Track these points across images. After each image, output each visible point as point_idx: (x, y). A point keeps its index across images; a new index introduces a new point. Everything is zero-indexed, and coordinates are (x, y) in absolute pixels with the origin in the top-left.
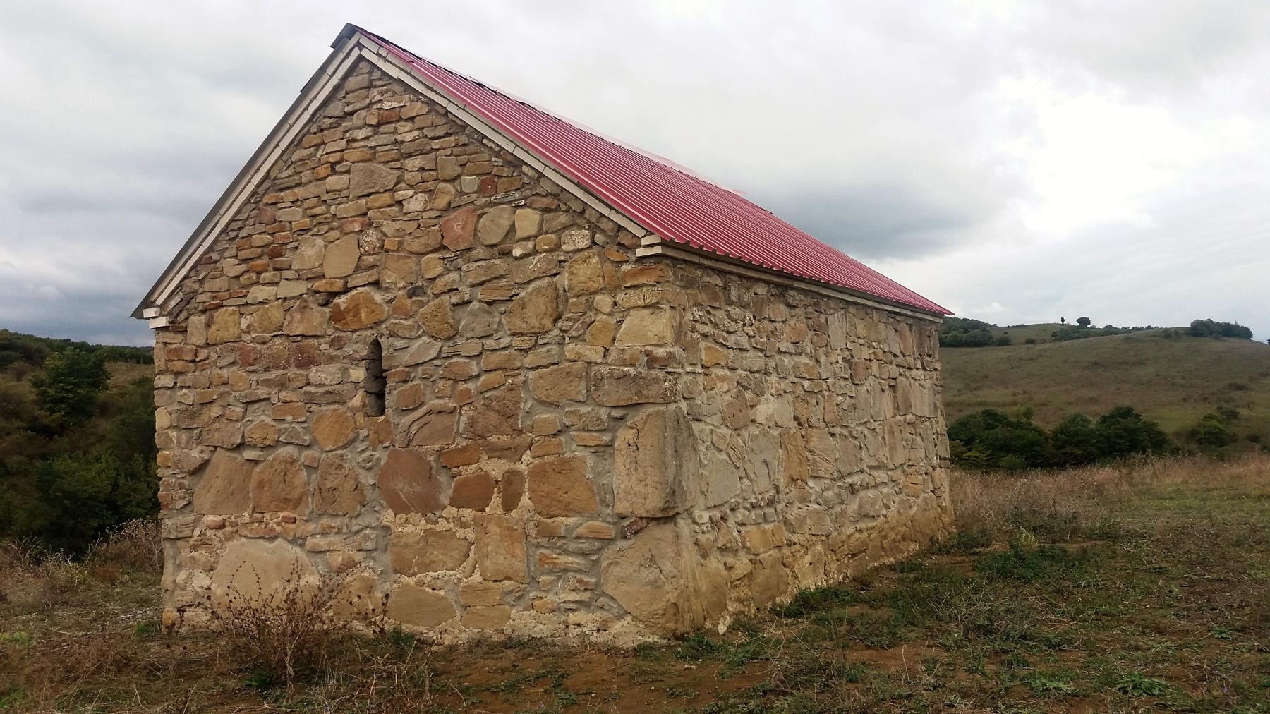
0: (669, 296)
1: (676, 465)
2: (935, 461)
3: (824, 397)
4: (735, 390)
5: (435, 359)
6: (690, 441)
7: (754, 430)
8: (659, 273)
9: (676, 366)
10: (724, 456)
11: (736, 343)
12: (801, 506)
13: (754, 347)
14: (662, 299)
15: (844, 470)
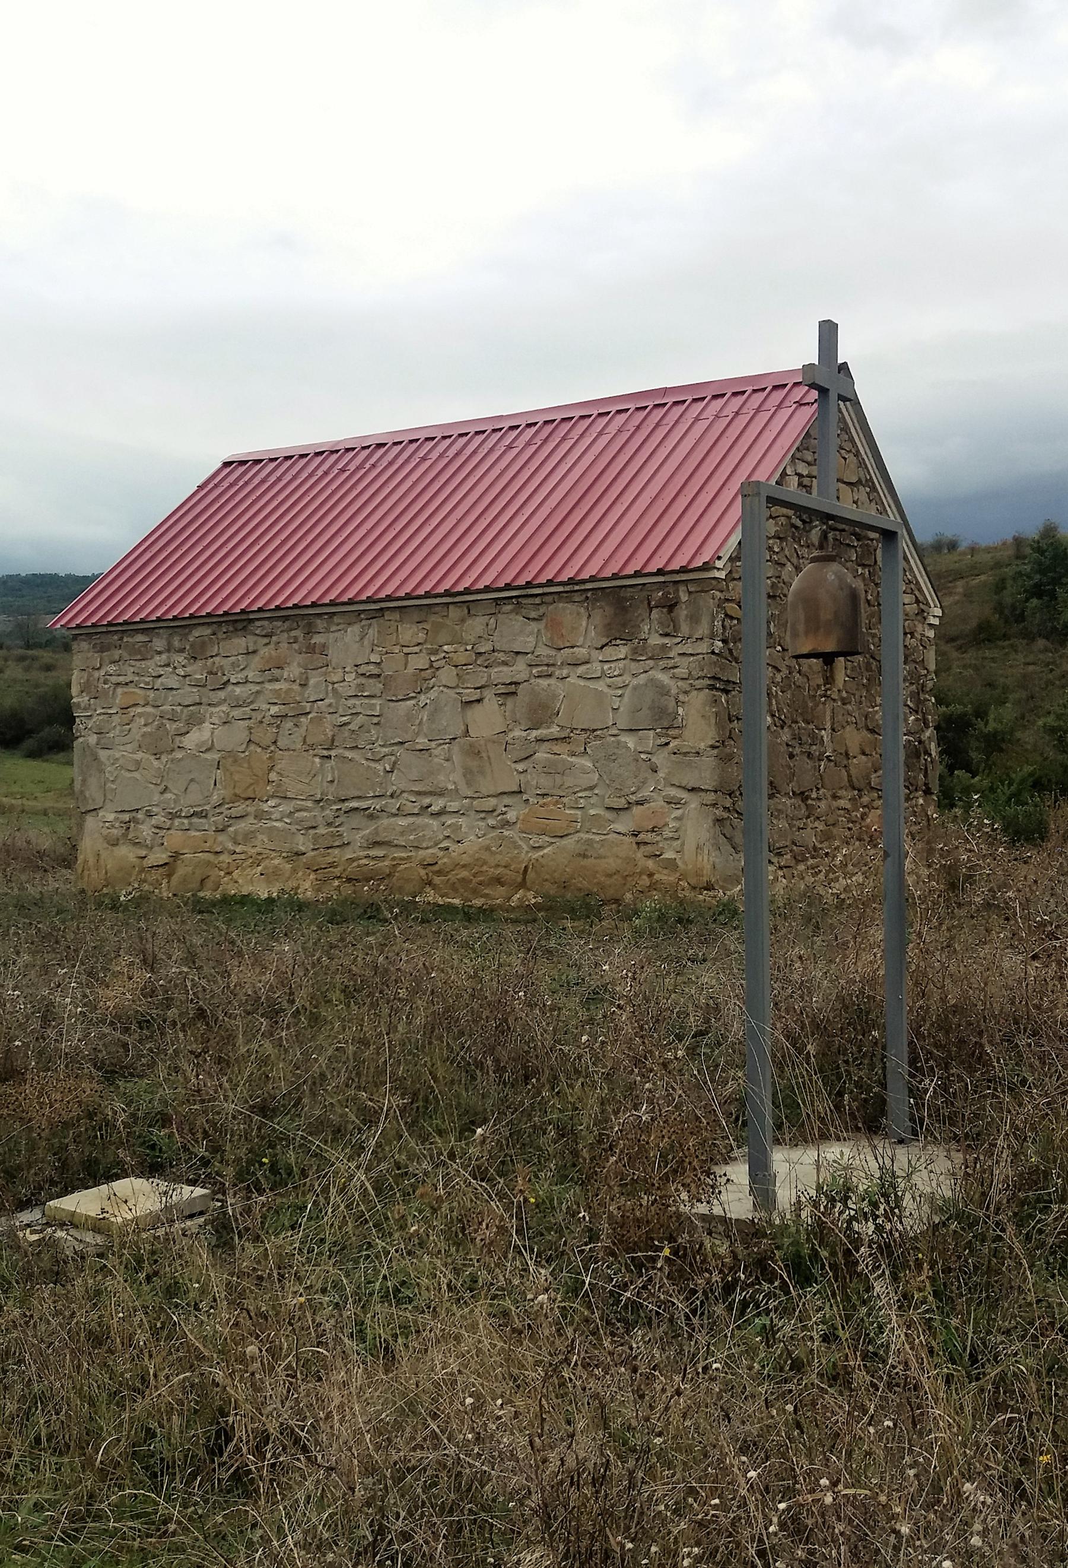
7: (179, 755)
11: (162, 684)
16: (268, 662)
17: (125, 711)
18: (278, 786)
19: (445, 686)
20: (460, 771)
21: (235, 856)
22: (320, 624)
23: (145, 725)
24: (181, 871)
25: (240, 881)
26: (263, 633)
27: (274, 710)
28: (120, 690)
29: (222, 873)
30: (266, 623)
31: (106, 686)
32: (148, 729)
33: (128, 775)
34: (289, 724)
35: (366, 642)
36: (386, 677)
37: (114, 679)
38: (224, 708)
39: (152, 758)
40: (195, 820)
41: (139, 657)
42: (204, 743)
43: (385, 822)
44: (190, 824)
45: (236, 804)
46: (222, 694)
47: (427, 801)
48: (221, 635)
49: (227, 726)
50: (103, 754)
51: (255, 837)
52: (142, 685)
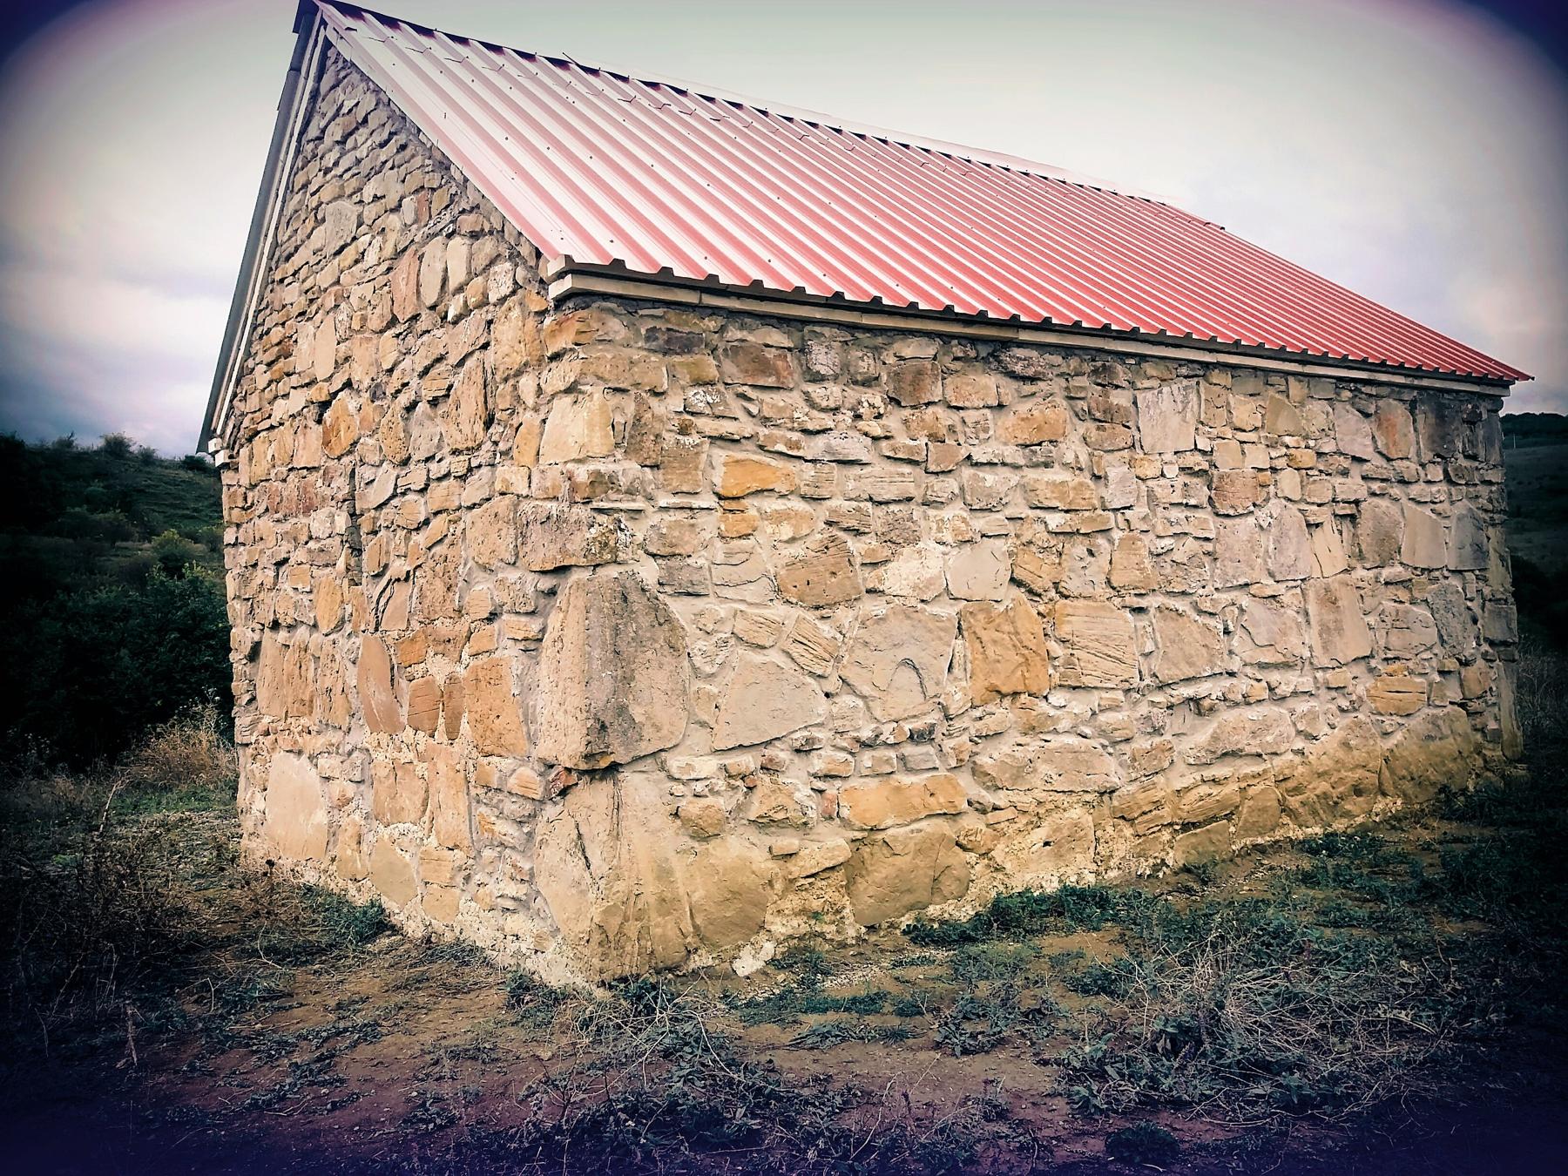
0: (604, 370)
1: (615, 678)
2: (1470, 648)
3: (1111, 541)
4: (819, 536)
5: (394, 496)
6: (662, 634)
8: (578, 326)
9: (615, 497)
10: (774, 656)
11: (829, 450)
12: (1022, 740)
13: (889, 457)
14: (583, 374)
15: (1166, 674)
16: (1039, 428)
17: (733, 505)
18: (1069, 664)
19: (1285, 498)
20: (1315, 628)
21: (992, 817)
22: (1121, 373)
23: (793, 540)
24: (882, 870)
25: (1008, 866)
26: (1030, 372)
27: (1055, 521)
28: (720, 454)
29: (971, 857)
30: (1034, 354)
31: (687, 440)
32: (797, 550)
33: (757, 658)
34: (1080, 549)
35: (1189, 415)
36: (1221, 478)
37: (708, 425)
38: (955, 511)
39: (811, 616)
40: (909, 750)
41: (771, 381)
42: (930, 583)
43: (1228, 716)
44: (902, 758)
45: (991, 708)
46: (951, 484)
47: (1274, 677)
48: (947, 361)
49: (968, 547)
50: (679, 608)
51: (1035, 770)
52: (781, 447)
